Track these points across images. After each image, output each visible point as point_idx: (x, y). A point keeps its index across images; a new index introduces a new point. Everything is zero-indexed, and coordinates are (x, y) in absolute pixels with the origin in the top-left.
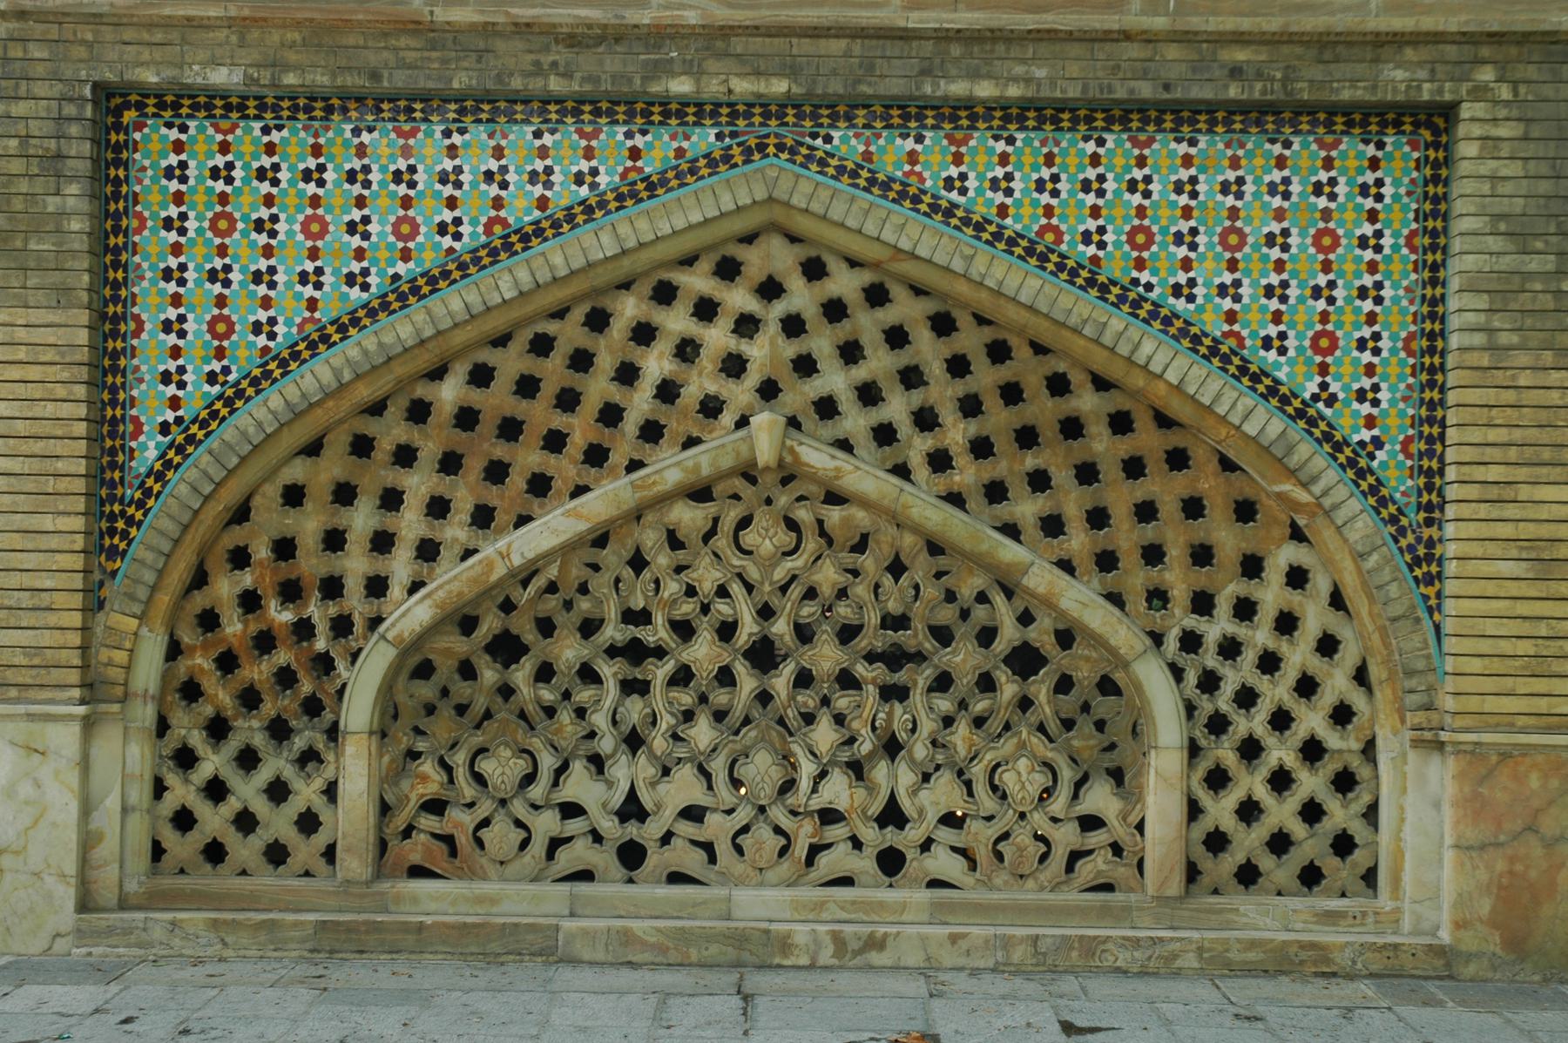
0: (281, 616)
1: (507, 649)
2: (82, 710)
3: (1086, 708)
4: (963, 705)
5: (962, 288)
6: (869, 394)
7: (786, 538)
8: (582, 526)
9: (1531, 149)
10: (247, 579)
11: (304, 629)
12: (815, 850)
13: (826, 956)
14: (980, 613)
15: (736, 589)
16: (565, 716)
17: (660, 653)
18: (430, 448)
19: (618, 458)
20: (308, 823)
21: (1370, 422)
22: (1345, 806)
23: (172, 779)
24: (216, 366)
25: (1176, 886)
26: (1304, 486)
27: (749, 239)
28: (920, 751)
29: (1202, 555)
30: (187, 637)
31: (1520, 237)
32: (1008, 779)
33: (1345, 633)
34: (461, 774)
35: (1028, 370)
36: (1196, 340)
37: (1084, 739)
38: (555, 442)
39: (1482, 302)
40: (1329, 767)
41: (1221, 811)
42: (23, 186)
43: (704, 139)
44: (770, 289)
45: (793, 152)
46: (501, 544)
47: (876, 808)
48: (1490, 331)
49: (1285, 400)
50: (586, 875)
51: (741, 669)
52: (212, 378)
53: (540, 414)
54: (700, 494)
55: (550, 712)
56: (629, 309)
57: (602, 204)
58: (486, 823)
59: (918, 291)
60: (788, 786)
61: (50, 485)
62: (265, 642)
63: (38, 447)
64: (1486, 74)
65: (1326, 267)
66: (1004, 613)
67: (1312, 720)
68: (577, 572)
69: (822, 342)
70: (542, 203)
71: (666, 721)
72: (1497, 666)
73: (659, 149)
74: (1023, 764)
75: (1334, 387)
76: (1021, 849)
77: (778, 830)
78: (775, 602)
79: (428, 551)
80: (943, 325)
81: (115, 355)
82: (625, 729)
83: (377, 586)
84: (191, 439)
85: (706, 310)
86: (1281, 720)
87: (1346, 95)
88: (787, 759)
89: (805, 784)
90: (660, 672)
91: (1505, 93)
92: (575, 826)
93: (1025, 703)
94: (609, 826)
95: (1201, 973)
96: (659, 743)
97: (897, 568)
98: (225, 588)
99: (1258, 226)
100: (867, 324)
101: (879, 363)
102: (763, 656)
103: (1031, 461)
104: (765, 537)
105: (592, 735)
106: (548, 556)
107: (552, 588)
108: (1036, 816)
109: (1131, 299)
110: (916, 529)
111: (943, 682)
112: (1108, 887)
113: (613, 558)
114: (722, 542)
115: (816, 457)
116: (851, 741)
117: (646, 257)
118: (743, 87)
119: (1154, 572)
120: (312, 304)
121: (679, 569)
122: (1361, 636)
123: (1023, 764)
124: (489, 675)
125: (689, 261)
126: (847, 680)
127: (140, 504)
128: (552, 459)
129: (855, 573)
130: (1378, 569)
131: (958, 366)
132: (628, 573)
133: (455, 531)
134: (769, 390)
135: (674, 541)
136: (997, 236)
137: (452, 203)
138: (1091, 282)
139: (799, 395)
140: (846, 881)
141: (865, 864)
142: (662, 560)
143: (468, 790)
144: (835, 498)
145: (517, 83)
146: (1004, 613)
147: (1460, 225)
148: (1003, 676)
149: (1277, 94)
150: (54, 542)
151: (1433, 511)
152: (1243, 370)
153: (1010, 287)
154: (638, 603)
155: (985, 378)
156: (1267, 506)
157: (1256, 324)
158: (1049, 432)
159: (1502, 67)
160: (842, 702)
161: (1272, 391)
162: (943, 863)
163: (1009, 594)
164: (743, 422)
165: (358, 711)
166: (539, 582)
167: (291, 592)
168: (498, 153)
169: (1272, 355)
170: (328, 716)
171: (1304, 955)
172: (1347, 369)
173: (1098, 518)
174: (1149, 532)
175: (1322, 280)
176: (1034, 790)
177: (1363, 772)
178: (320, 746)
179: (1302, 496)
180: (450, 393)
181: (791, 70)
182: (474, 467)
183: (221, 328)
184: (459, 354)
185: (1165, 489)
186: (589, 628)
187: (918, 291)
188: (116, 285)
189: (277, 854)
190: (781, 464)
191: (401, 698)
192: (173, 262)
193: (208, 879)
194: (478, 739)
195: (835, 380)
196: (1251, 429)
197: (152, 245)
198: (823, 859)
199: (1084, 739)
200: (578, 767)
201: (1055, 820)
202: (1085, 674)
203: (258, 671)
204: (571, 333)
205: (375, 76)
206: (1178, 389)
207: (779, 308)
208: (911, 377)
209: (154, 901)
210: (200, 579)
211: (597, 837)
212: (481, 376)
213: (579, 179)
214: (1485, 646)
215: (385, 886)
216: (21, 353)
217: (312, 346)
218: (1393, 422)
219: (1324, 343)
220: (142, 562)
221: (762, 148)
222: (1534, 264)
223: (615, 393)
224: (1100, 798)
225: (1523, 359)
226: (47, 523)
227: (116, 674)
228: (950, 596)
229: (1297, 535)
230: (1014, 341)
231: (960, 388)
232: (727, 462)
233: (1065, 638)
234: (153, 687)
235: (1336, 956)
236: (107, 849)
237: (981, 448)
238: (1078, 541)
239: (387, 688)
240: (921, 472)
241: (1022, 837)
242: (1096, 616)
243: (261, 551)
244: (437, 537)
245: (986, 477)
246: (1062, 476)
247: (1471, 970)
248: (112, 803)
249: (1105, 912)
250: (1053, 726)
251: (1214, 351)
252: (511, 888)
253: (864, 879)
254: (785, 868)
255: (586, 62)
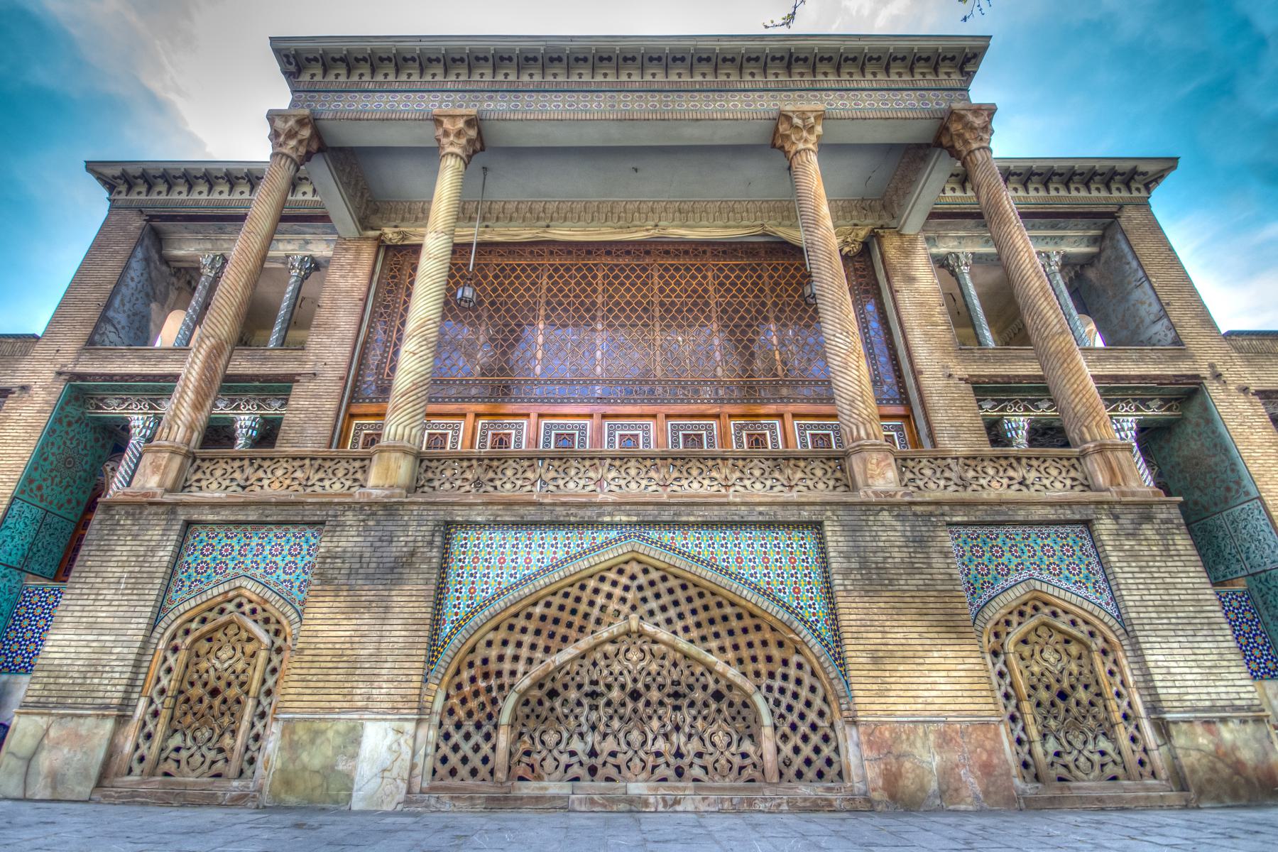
0: (482, 684)
1: (553, 694)
2: (416, 717)
3: (739, 713)
4: (699, 712)
5: (689, 576)
6: (664, 609)
7: (640, 655)
8: (578, 652)
9: (845, 533)
10: (473, 672)
11: (489, 689)
12: (654, 767)
13: (661, 808)
14: (702, 679)
15: (625, 672)
16: (571, 719)
17: (602, 695)
18: (531, 627)
19: (589, 630)
20: (485, 760)
21: (814, 614)
22: (828, 747)
23: (442, 744)
24: (470, 602)
25: (776, 780)
26: (798, 635)
27: (626, 563)
28: (687, 729)
29: (769, 659)
30: (452, 692)
31: (848, 558)
32: (716, 739)
33: (818, 685)
34: (537, 740)
35: (711, 601)
36: (759, 590)
37: (739, 724)
38: (570, 625)
39: (840, 577)
40: (820, 733)
41: (787, 749)
42: (422, 550)
43: (613, 534)
44: (633, 577)
45: (639, 537)
46: (553, 658)
47: (673, 751)
48: (845, 585)
49: (788, 608)
50: (577, 779)
51: (628, 700)
52: (468, 606)
53: (565, 616)
54: (613, 641)
55: (566, 717)
56: (592, 584)
57: (585, 553)
58: (544, 760)
59: (676, 577)
60: (644, 743)
61: (417, 639)
62: (476, 694)
63: (415, 627)
64: (829, 513)
65: (794, 568)
66: (710, 680)
67: (812, 716)
68: (576, 667)
69: (649, 593)
70: (567, 553)
71: (604, 719)
72: (867, 693)
73: (601, 537)
74: (720, 733)
75: (802, 604)
76: (723, 766)
77: (642, 760)
78: (638, 676)
79: (530, 661)
80: (684, 587)
81: (440, 599)
82: (591, 723)
83: (513, 673)
84: (460, 625)
85: (614, 584)
86: (802, 716)
87: (792, 519)
88: (644, 733)
89: (650, 742)
90: (602, 702)
91: (835, 518)
92: (574, 759)
93: (719, 711)
94: (585, 759)
95: (789, 812)
96: (602, 728)
97: (675, 665)
98: (465, 675)
99: (773, 556)
100: (662, 587)
101: (666, 599)
102: (635, 695)
103: (714, 629)
104: (634, 655)
105: (580, 725)
106: (567, 662)
107: (568, 673)
108: (727, 753)
109: (738, 577)
110: (680, 651)
111: (692, 704)
112: (753, 780)
113: (587, 662)
114: (621, 657)
115: (648, 627)
116: (664, 726)
117: (597, 568)
118: (624, 519)
119: (755, 665)
120: (500, 583)
121: (608, 666)
122: (823, 686)
123: (720, 733)
124: (547, 704)
125: (609, 569)
126: (661, 703)
127: (443, 647)
128: (569, 630)
129: (662, 666)
130: (824, 662)
131: (689, 600)
132: (592, 668)
133: (539, 655)
134: (634, 608)
135: (606, 657)
136: (698, 560)
137: (542, 553)
138: (727, 573)
139: (643, 609)
140: (665, 780)
141: (670, 773)
142: (602, 663)
143: (539, 747)
144: (655, 642)
145: (562, 519)
146: (710, 680)
147: (832, 554)
148: (711, 701)
149: (773, 519)
150: (415, 659)
151: (839, 641)
152: (774, 599)
153: (704, 574)
154: (595, 677)
155: (698, 603)
156: (787, 642)
157: (776, 585)
158: (718, 619)
159: (833, 511)
160: (661, 712)
161: (784, 605)
162: (697, 772)
163: (711, 673)
164: (626, 617)
165: (505, 718)
166: (564, 671)
167: (486, 676)
168: (555, 539)
169: (782, 594)
170: (494, 720)
171: (824, 803)
172: (804, 598)
173: (736, 647)
174: (752, 652)
175: (793, 572)
176: (725, 743)
177: (832, 735)
178: (491, 731)
179: (797, 638)
180: (538, 610)
181: (638, 515)
182: (545, 634)
183: (472, 591)
184: (542, 598)
185: (755, 637)
186: (580, 686)
187: (676, 577)
188: (443, 578)
189: (474, 772)
190: (638, 631)
191: (519, 713)
192: (460, 571)
193: (450, 782)
194: (543, 727)
195: (653, 604)
196: (779, 617)
197: (455, 566)
198: (657, 771)
199: (739, 724)
200: (575, 737)
201: (733, 754)
202: (737, 700)
203: (473, 704)
204: (575, 591)
205: (522, 517)
206: (756, 605)
207: (636, 583)
208: (676, 603)
209: (433, 789)
210: (458, 672)
211: (581, 764)
212: (548, 605)
213: (578, 546)
214: (862, 687)
215: (509, 783)
216: (414, 599)
217: (499, 595)
218: (821, 614)
219: (796, 591)
220: (440, 666)
221: (630, 536)
222: (853, 566)
223: (588, 609)
224: (747, 746)
225: (856, 594)
226: (414, 652)
227: (428, 705)
228: (692, 674)
229: (798, 652)
230: (705, 591)
231: (690, 606)
232: (622, 630)
233: (730, 687)
234: (440, 711)
235: (834, 803)
236: (418, 771)
237: (698, 625)
238: (730, 655)
239: (514, 709)
240: (681, 633)
241: (723, 761)
242: (739, 680)
243: (478, 662)
244: (532, 656)
245: (701, 634)
246: (723, 633)
247: (879, 808)
248: (422, 752)
249: (752, 790)
250: (729, 720)
251: (765, 593)
252: (552, 784)
253: (672, 778)
254: (644, 775)
255: (581, 513)
